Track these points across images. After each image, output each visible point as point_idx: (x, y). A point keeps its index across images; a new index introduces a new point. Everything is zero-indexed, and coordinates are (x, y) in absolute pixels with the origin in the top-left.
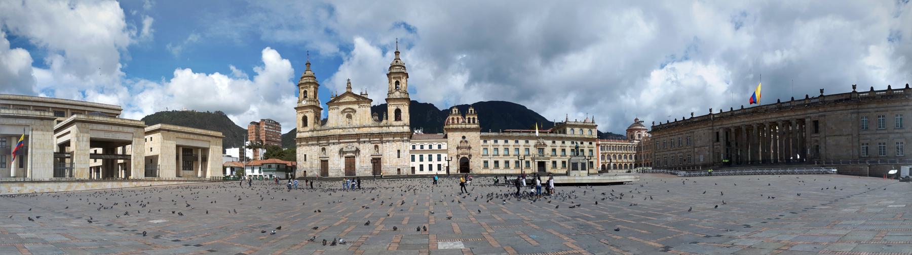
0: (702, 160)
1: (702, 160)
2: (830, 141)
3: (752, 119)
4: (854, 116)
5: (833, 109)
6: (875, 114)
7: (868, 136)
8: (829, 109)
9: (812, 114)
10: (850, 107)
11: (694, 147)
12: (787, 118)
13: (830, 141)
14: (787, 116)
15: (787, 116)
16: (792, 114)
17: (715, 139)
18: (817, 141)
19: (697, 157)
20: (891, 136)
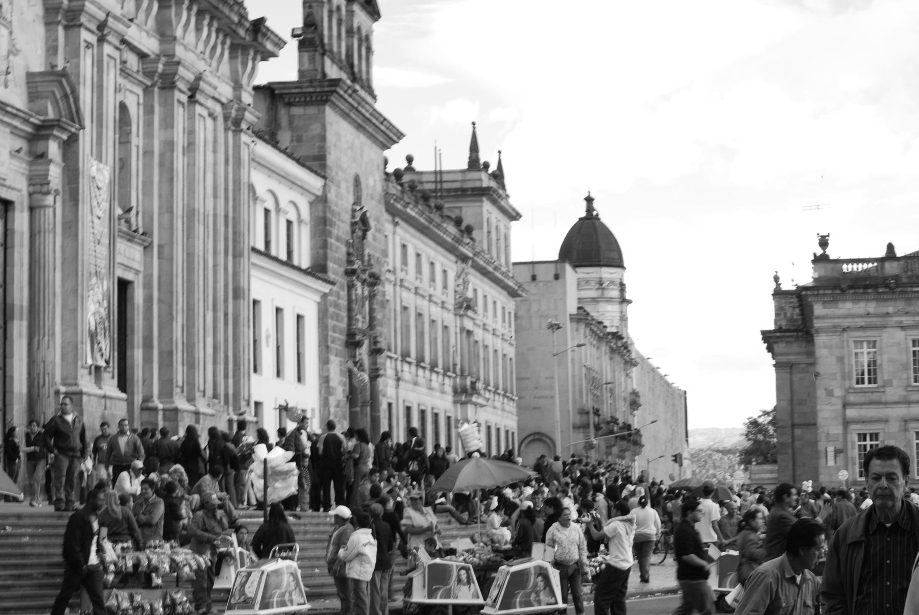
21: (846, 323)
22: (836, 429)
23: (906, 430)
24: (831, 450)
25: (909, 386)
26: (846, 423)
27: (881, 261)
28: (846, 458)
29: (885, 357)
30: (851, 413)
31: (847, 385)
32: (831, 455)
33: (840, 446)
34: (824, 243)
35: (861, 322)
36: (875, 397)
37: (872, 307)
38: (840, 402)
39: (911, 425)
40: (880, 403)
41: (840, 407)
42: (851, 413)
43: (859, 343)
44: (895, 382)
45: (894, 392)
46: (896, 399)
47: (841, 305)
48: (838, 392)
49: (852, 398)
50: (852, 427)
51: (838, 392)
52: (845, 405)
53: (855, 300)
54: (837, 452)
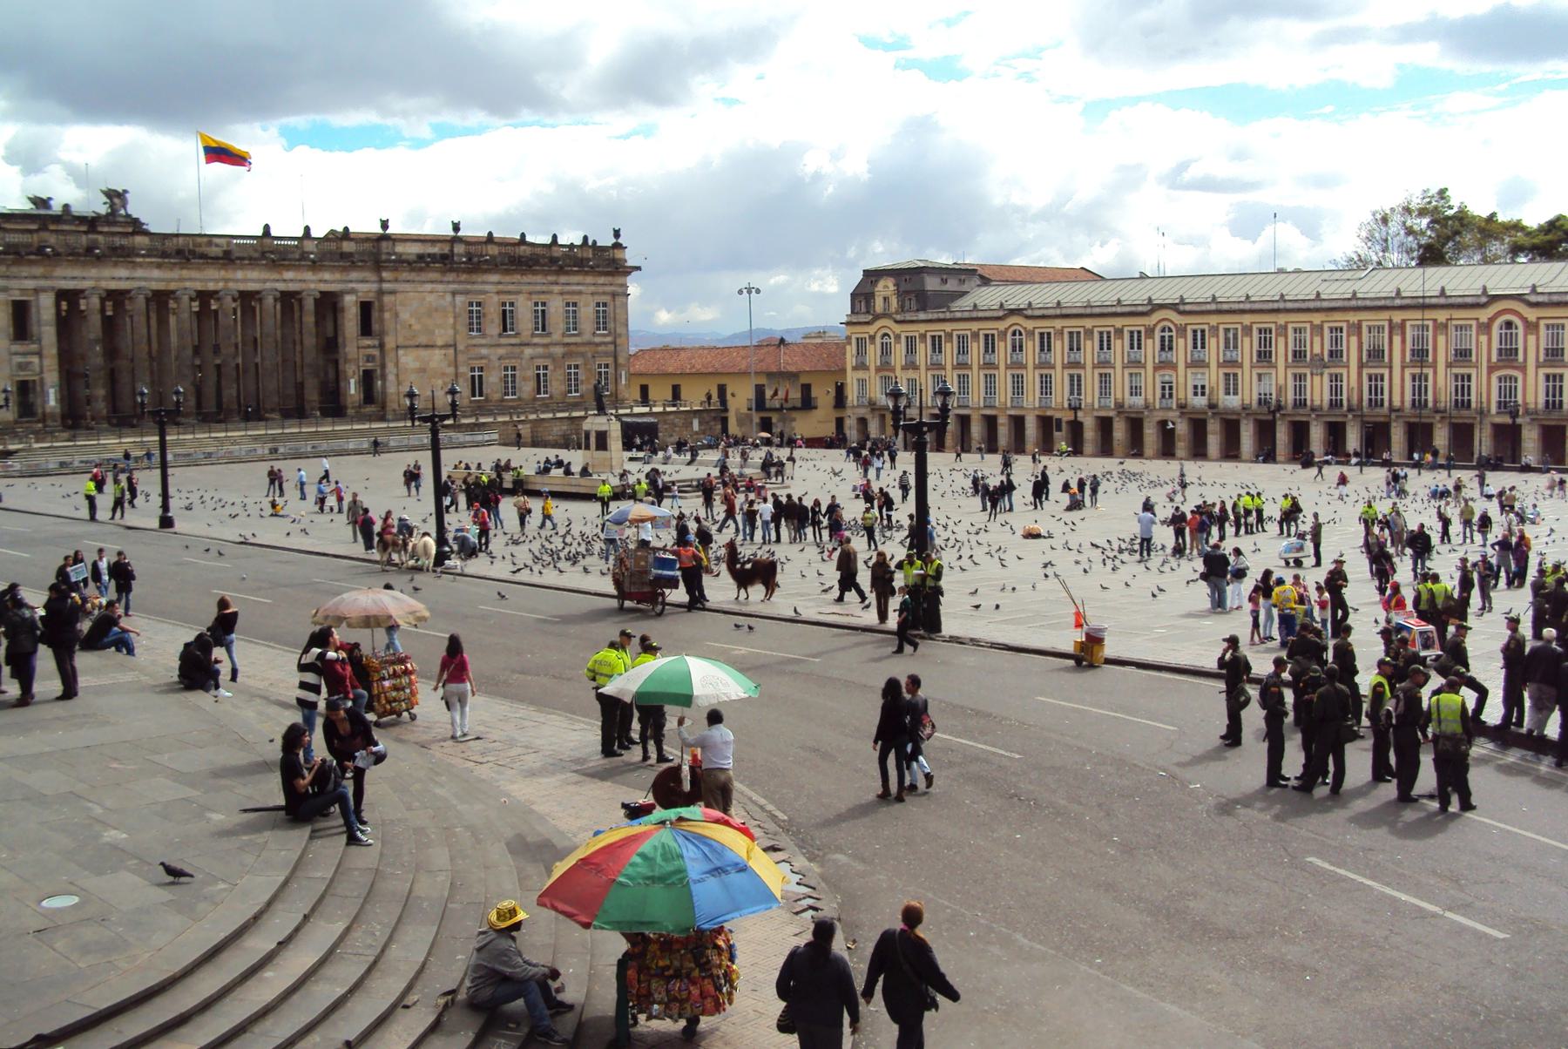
2: (409, 359)
3: (176, 274)
4: (459, 299)
5: (412, 276)
6: (496, 298)
7: (484, 351)
8: (405, 275)
9: (356, 287)
10: (451, 277)
12: (292, 287)
13: (409, 359)
14: (290, 280)
15: (290, 280)
16: (309, 275)
18: (370, 358)
20: (528, 351)
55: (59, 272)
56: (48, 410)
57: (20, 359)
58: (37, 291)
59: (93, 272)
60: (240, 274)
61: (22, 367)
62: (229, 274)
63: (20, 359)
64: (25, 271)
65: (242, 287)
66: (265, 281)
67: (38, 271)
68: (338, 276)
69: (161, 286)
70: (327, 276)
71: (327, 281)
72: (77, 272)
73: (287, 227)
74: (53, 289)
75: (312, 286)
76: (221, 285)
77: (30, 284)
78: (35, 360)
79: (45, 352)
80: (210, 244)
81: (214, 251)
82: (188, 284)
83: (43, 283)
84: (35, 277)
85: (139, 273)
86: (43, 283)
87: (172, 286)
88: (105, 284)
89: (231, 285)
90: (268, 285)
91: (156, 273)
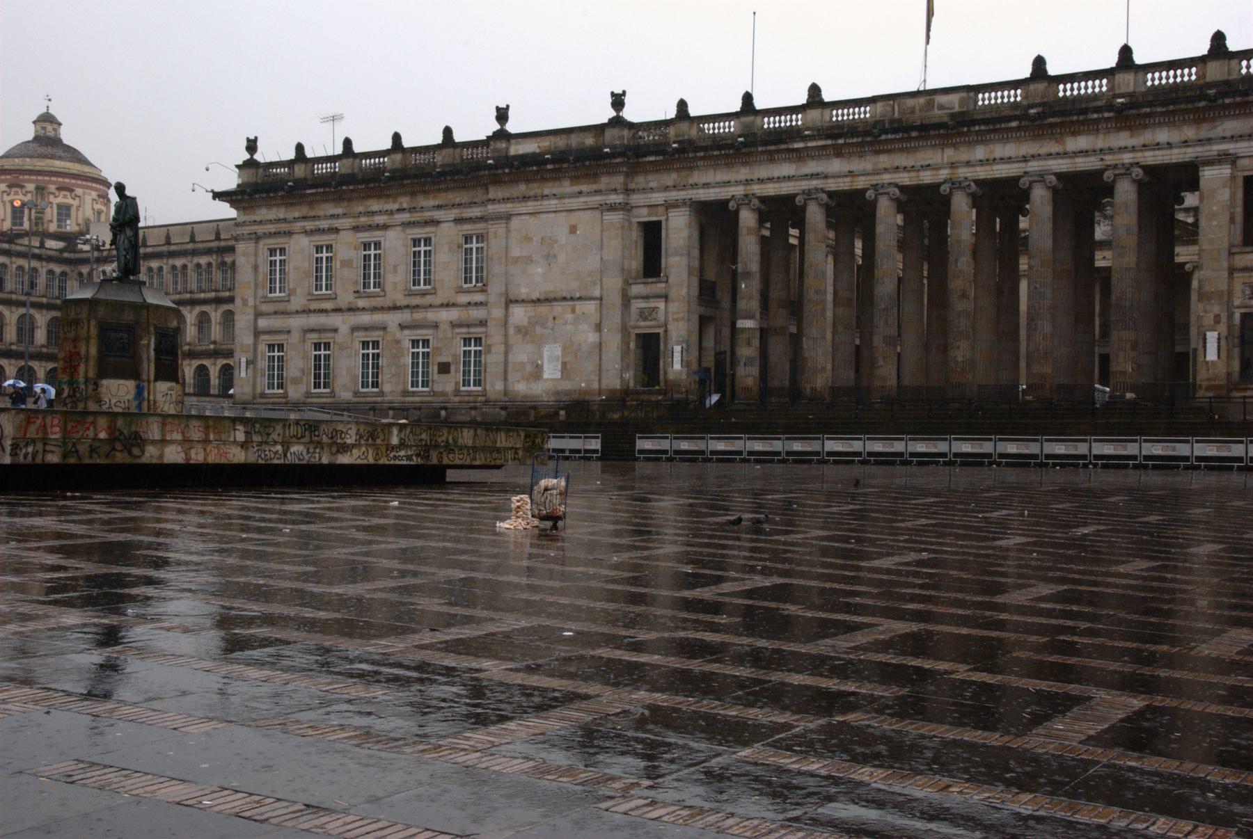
0: (551, 371)
1: (551, 371)
3: (866, 164)
11: (509, 302)
12: (1083, 164)
14: (1079, 152)
15: (1079, 152)
16: (1123, 139)
17: (636, 263)
19: (522, 354)
21: (260, 229)
22: (248, 339)
23: (304, 341)
24: (244, 360)
25: (310, 294)
26: (257, 333)
27: (289, 164)
28: (255, 370)
29: (292, 265)
30: (263, 323)
31: (260, 293)
32: (243, 365)
33: (250, 358)
34: (252, 146)
35: (272, 228)
36: (281, 307)
37: (281, 213)
38: (252, 311)
39: (309, 336)
40: (283, 313)
41: (252, 317)
42: (263, 323)
43: (272, 252)
44: (299, 291)
45: (297, 302)
46: (299, 308)
47: (257, 212)
48: (251, 303)
49: (265, 308)
50: (263, 337)
51: (251, 303)
52: (258, 314)
53: (269, 206)
54: (248, 363)
55: (696, 177)
56: (671, 376)
57: (641, 304)
58: (669, 206)
59: (743, 173)
60: (980, 152)
61: (644, 315)
62: (963, 155)
63: (641, 304)
64: (653, 180)
65: (983, 173)
66: (1025, 159)
67: (670, 178)
68: (1189, 132)
69: (844, 185)
70: (1162, 135)
71: (1166, 144)
72: (721, 176)
73: (1081, 51)
74: (684, 203)
75: (1127, 158)
76: (944, 174)
77: (658, 198)
78: (661, 305)
79: (672, 294)
80: (930, 105)
81: (937, 114)
82: (887, 178)
83: (674, 195)
84: (667, 188)
85: (812, 167)
86: (674, 195)
87: (861, 183)
88: (757, 189)
89: (963, 172)
90: (1033, 166)
91: (836, 165)
